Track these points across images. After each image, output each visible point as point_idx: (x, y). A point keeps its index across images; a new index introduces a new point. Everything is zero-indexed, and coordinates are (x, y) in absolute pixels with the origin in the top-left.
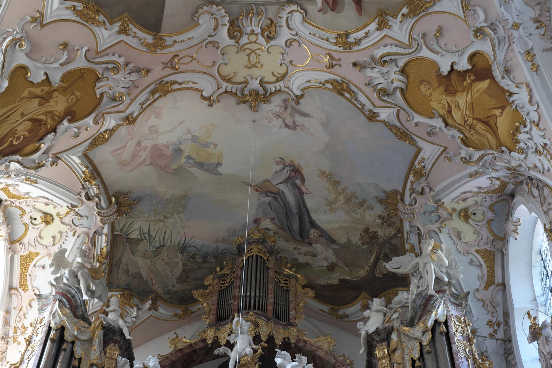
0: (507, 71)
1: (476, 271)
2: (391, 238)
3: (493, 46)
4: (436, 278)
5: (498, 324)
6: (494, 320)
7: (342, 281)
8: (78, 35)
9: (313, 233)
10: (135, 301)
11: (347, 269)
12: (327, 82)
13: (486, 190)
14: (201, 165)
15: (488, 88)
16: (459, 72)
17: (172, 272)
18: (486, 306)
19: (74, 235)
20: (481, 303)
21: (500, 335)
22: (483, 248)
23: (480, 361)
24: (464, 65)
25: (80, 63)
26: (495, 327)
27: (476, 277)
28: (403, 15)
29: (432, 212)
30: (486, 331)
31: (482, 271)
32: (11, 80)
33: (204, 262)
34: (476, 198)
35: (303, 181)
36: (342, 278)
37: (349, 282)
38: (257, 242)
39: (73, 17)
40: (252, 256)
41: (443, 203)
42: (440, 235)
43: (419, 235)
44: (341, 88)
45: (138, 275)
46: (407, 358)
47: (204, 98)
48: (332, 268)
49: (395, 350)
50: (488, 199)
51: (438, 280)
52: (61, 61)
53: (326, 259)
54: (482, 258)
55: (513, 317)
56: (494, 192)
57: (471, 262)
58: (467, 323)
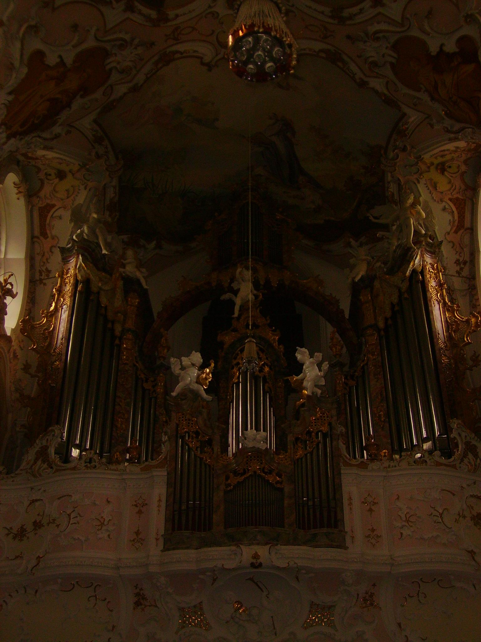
1: (448, 217)
5: (465, 263)
13: (462, 149)
18: (455, 247)
20: (451, 244)
21: (465, 272)
22: (455, 196)
23: (449, 304)
26: (462, 266)
29: (412, 166)
30: (453, 269)
31: (454, 217)
34: (453, 155)
41: (423, 158)
42: (418, 185)
43: (399, 184)
44: (334, 57)
47: (203, 64)
50: (463, 155)
51: (417, 232)
54: (455, 205)
56: (469, 150)
57: (444, 209)
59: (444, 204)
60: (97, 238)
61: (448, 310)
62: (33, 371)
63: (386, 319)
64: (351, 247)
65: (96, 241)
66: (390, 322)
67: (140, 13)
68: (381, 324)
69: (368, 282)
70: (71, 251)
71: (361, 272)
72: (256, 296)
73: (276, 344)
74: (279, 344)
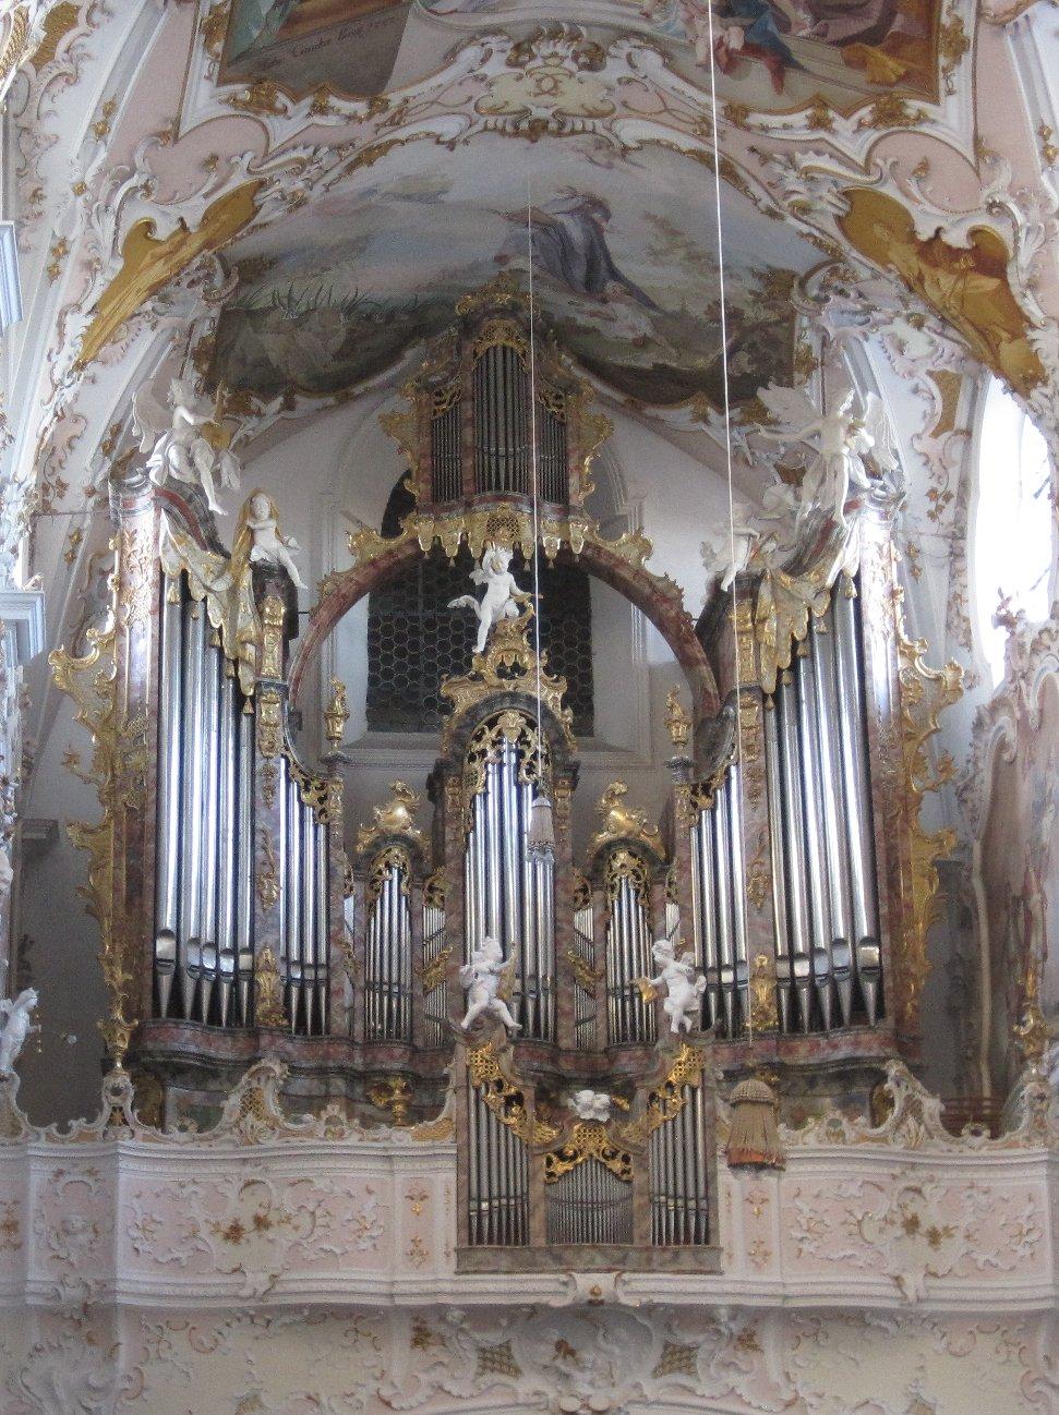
0: (1032, 285)
1: (921, 405)
2: (769, 325)
3: (1016, 233)
4: (850, 481)
5: (948, 497)
6: (941, 490)
7: (661, 369)
8: (240, 140)
9: (611, 286)
10: (256, 402)
11: (673, 351)
12: (691, 152)
14: (408, 197)
15: (996, 291)
16: (949, 248)
17: (325, 346)
19: (153, 328)
20: (923, 459)
24: (957, 238)
25: (238, 180)
26: (941, 502)
27: (920, 416)
28: (860, 125)
31: (933, 408)
32: (127, 255)
33: (387, 323)
35: (607, 216)
36: (661, 362)
37: (673, 371)
38: (503, 312)
39: (227, 110)
40: (495, 348)
42: (865, 344)
45: (264, 362)
46: (784, 632)
48: (642, 344)
49: (763, 620)
51: (854, 486)
52: (204, 191)
53: (633, 329)
55: (975, 514)
57: (916, 391)
58: (893, 556)
59: (915, 380)
60: (197, 474)
61: (902, 653)
62: (85, 767)
63: (780, 671)
64: (707, 422)
65: (194, 481)
66: (786, 678)
67: (338, 112)
68: (769, 685)
69: (750, 585)
70: (138, 490)
71: (737, 559)
72: (522, 607)
73: (558, 712)
74: (564, 707)
